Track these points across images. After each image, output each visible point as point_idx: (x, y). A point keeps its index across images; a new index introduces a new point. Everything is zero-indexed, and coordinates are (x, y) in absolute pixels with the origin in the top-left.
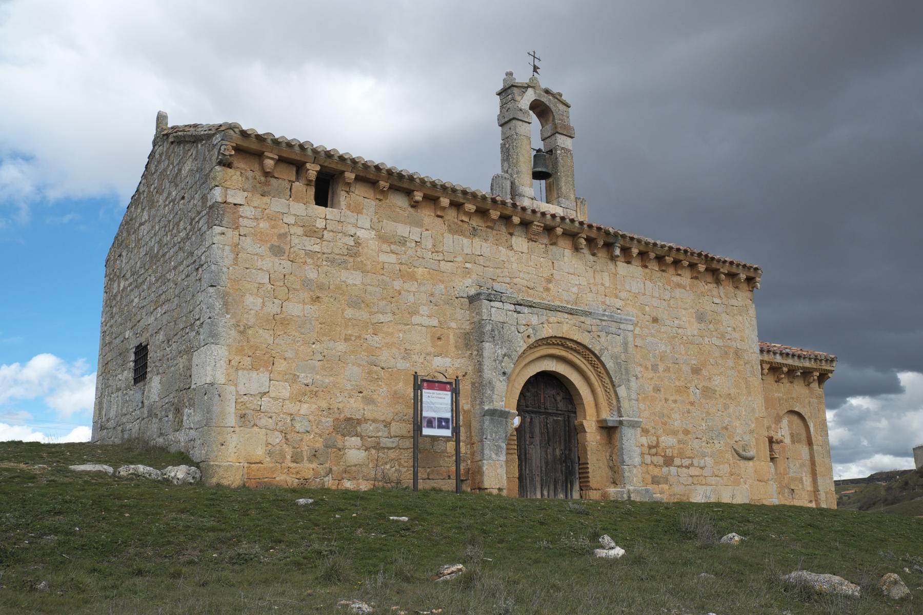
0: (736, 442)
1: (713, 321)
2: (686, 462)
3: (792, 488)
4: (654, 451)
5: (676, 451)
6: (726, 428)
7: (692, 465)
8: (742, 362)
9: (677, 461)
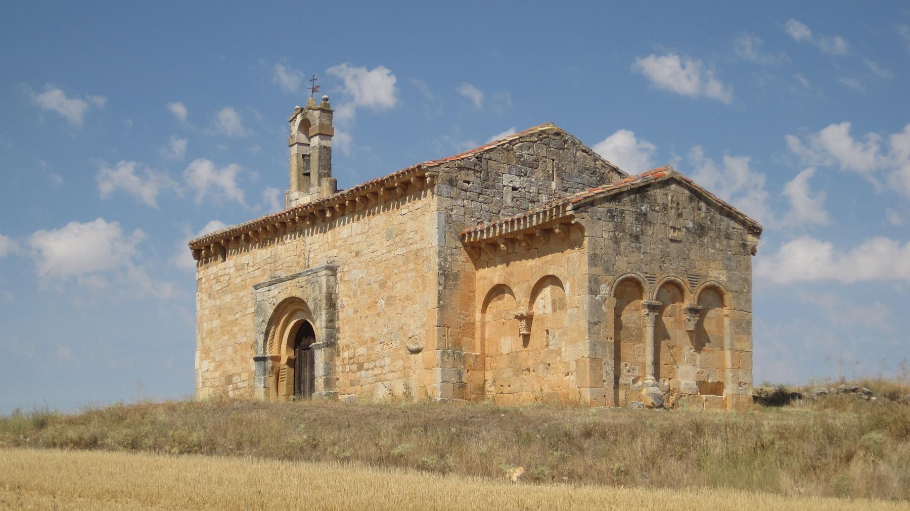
0: (410, 338)
1: (399, 233)
2: (371, 365)
3: (548, 362)
4: (352, 361)
5: (365, 358)
6: (402, 328)
7: (375, 366)
8: (421, 261)
9: (366, 366)
